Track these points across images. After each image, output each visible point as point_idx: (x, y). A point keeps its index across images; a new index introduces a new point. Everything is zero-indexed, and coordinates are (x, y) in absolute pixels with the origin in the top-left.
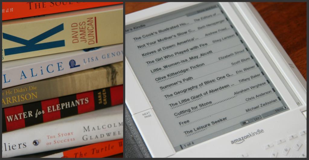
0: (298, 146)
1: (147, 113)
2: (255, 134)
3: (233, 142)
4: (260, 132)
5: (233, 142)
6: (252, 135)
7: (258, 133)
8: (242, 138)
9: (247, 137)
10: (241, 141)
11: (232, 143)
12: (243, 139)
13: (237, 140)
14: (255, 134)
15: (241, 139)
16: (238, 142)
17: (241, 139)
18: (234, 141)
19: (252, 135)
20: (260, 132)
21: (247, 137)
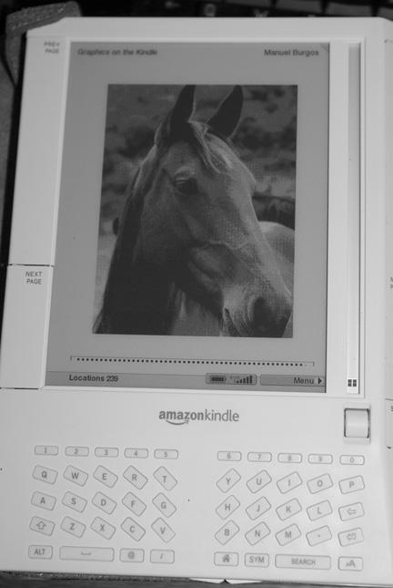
0: (289, 484)
1: (36, 274)
2: (218, 416)
3: (163, 415)
4: (232, 417)
5: (163, 415)
6: (210, 416)
7: (225, 417)
8: (188, 414)
9: (199, 416)
10: (182, 421)
11: (160, 418)
12: (186, 418)
13: (175, 413)
14: (218, 416)
15: (185, 415)
16: (173, 421)
17: (185, 415)
18: (168, 413)
19: (210, 416)
20: (232, 417)
21: (199, 416)
